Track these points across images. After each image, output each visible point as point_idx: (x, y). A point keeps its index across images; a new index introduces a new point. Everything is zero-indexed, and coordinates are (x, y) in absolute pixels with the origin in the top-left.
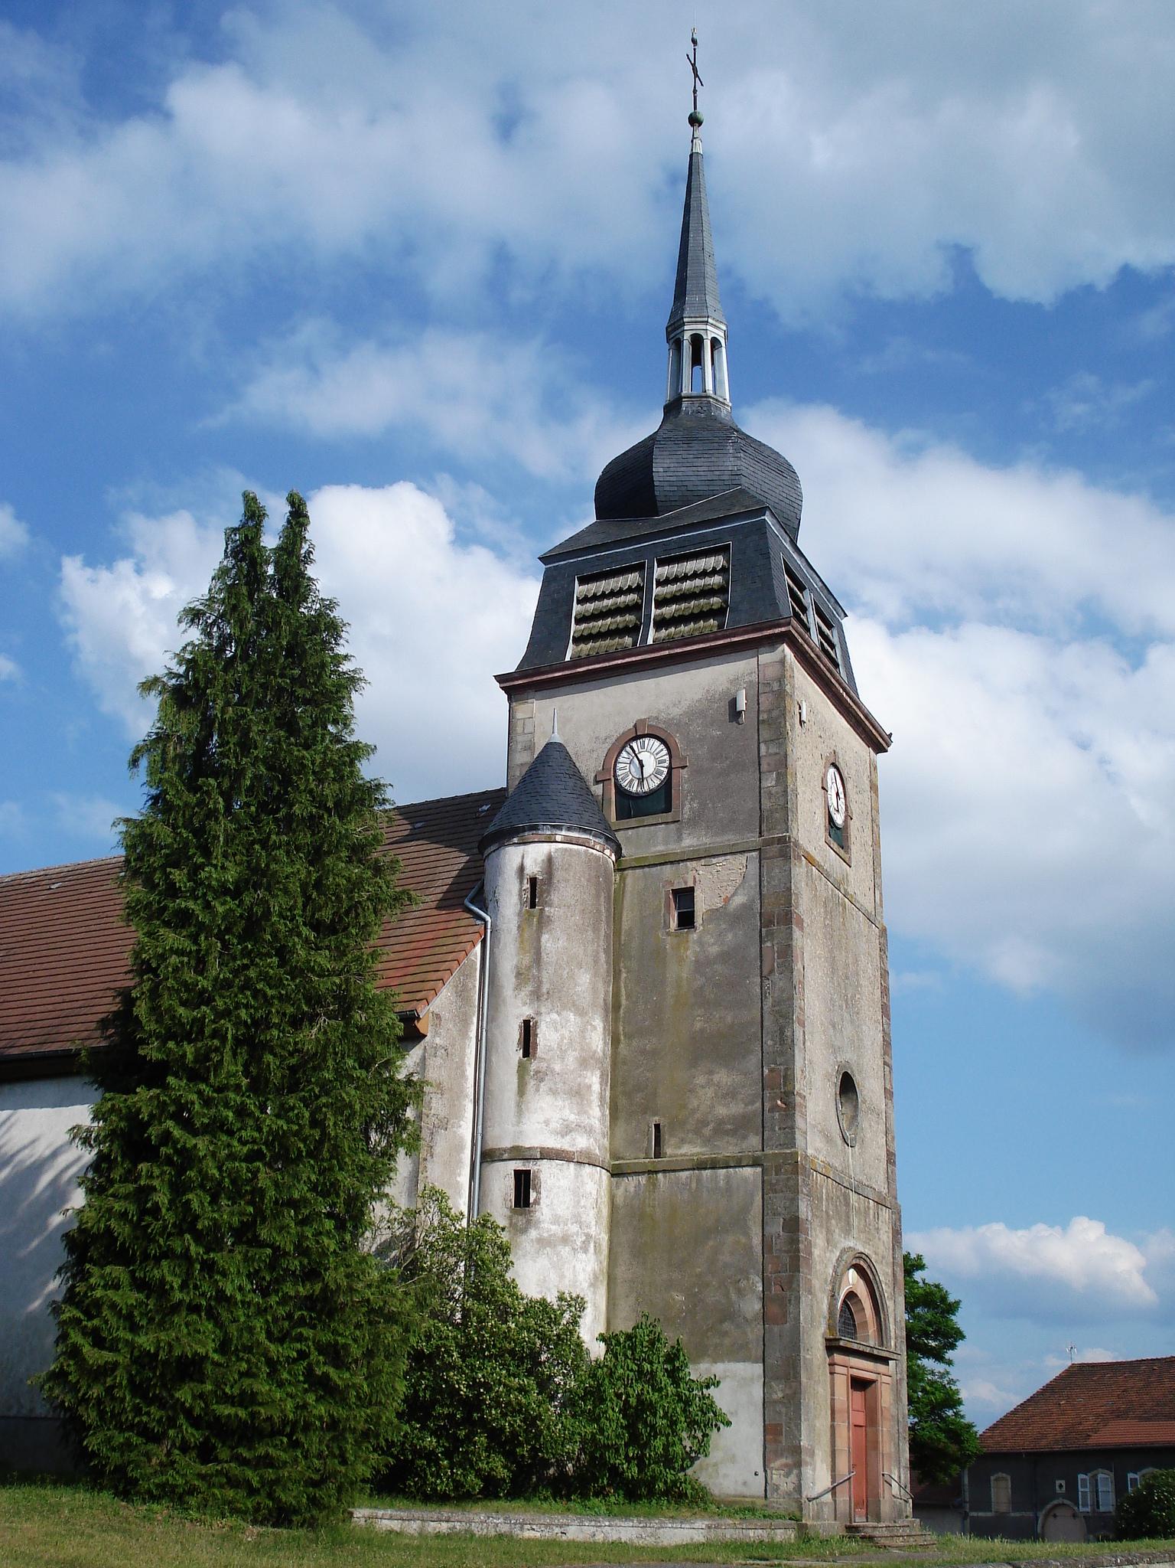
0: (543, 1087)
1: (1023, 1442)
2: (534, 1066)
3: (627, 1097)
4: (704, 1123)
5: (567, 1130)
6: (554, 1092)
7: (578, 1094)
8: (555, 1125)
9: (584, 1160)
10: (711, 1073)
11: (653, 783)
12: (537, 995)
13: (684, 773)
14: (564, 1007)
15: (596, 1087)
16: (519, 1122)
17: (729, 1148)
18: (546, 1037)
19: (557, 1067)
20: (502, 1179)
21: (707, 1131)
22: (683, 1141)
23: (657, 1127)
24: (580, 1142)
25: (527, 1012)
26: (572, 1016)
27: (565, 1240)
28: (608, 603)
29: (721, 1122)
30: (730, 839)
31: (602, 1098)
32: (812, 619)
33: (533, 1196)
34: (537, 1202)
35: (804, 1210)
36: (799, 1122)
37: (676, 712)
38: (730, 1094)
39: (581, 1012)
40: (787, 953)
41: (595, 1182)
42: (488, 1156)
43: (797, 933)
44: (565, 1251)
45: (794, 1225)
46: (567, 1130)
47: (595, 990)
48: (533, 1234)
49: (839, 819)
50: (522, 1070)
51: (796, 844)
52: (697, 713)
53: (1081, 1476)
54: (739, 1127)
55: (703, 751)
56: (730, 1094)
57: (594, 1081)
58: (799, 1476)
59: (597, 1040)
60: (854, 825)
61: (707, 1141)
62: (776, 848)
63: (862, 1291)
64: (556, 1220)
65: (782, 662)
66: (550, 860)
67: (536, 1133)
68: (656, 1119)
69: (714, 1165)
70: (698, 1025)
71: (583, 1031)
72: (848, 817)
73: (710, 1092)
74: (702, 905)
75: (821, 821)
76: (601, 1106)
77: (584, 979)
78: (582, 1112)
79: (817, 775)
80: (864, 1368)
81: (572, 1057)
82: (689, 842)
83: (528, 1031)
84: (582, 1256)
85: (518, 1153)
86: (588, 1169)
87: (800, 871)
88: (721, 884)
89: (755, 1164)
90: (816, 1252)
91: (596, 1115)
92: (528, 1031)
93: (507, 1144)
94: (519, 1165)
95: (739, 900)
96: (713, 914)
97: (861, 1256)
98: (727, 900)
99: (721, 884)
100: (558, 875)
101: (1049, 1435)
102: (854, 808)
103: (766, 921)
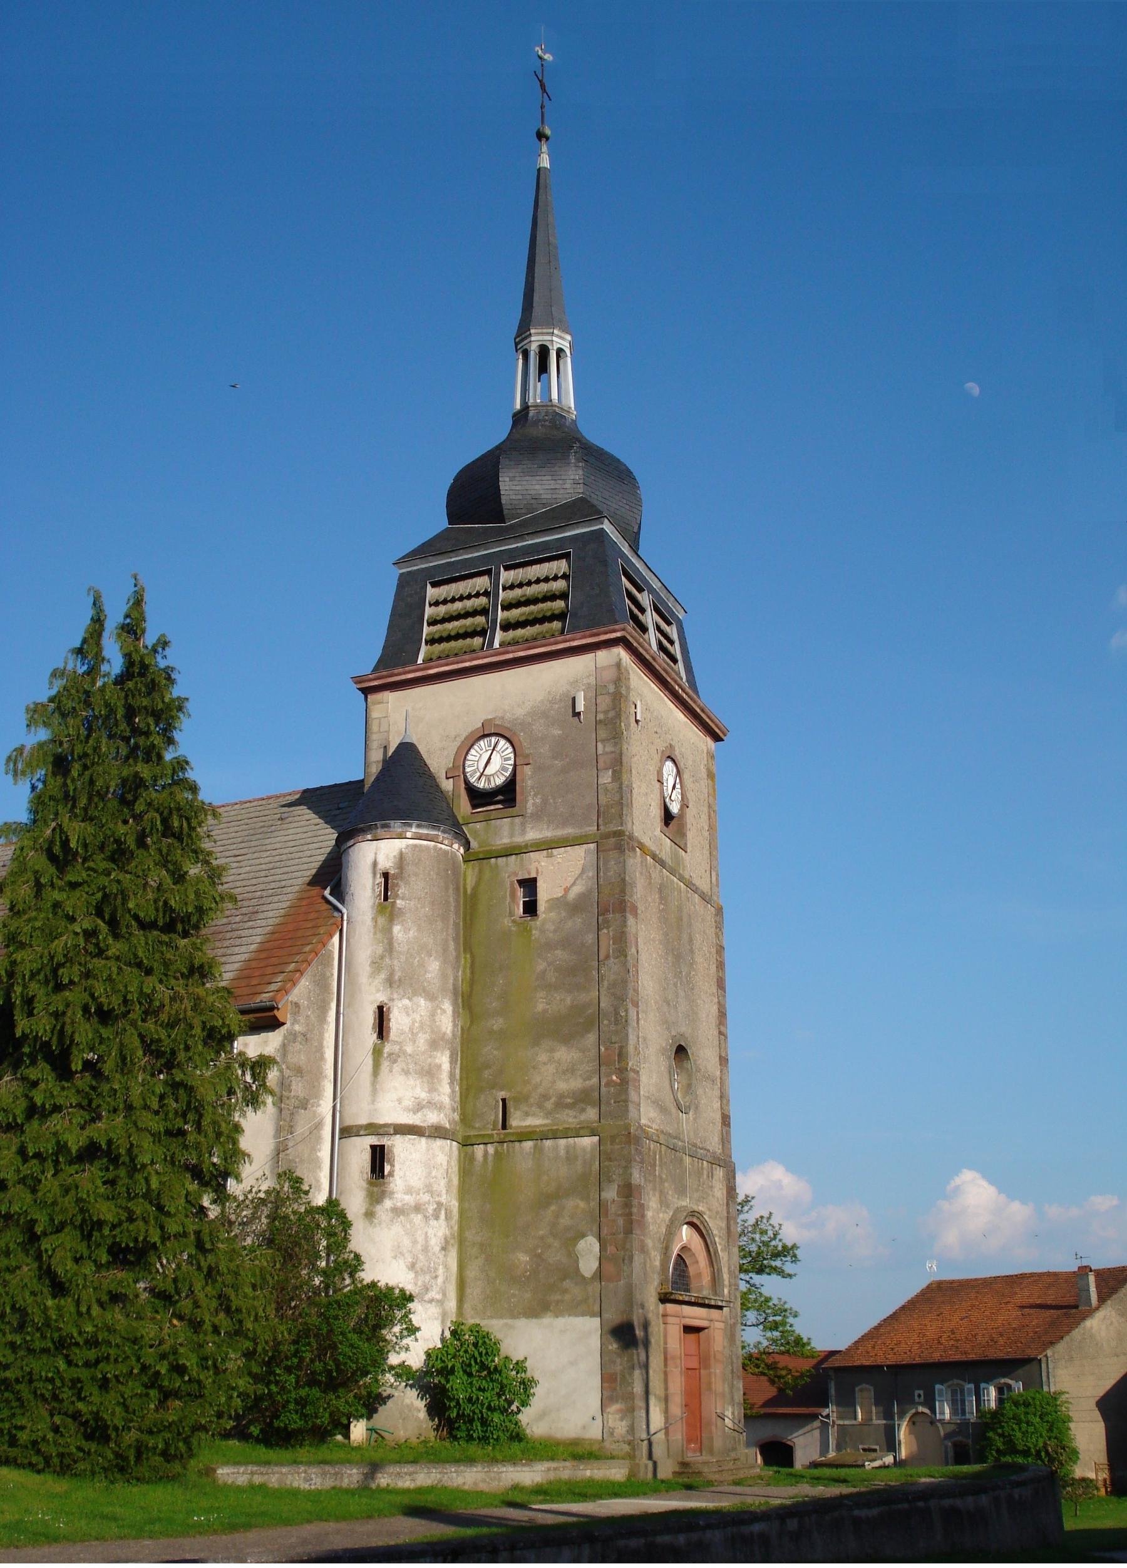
0: (396, 1068)
1: (883, 1356)
2: (388, 1048)
3: (472, 1077)
4: (545, 1097)
5: (419, 1107)
6: (406, 1072)
7: (429, 1073)
8: (408, 1102)
9: (437, 1132)
10: (552, 1050)
11: (499, 781)
12: (390, 982)
13: (528, 770)
14: (415, 993)
15: (446, 1066)
16: (373, 1102)
17: (569, 1118)
18: (398, 1021)
19: (409, 1049)
20: (359, 1152)
21: (549, 1105)
22: (527, 1114)
23: (504, 1100)
24: (432, 1118)
25: (381, 997)
26: (422, 1002)
27: (418, 1208)
28: (458, 605)
29: (561, 1096)
30: (569, 831)
31: (452, 1075)
32: (650, 618)
33: (387, 1168)
34: (391, 1174)
35: (637, 1177)
36: (633, 1096)
37: (520, 712)
38: (571, 1070)
39: (431, 997)
40: (622, 940)
41: (444, 1153)
42: (347, 1132)
43: (631, 921)
44: (418, 1219)
45: (628, 1191)
46: (419, 1107)
47: (444, 976)
48: (388, 1203)
49: (675, 808)
50: (377, 1053)
51: (631, 837)
52: (540, 713)
53: (938, 1387)
54: (582, 1099)
55: (545, 750)
56: (571, 1070)
57: (444, 1060)
58: (633, 1418)
59: (446, 1022)
60: (690, 813)
61: (548, 1114)
62: (612, 840)
63: (697, 1244)
64: (409, 1191)
65: (618, 665)
66: (401, 858)
67: (391, 1111)
68: (502, 1094)
69: (555, 1135)
70: (540, 1007)
71: (433, 1015)
72: (684, 805)
73: (551, 1068)
74: (544, 894)
75: (657, 813)
76: (451, 1083)
77: (434, 966)
78: (432, 1089)
79: (652, 769)
80: (695, 1315)
81: (422, 1039)
82: (532, 835)
83: (382, 1015)
84: (433, 1223)
85: (372, 1129)
86: (439, 1142)
87: (635, 862)
88: (562, 874)
89: (593, 1134)
90: (649, 1214)
91: (446, 1093)
92: (382, 1015)
93: (363, 1121)
94: (374, 1140)
95: (577, 890)
96: (555, 903)
97: (693, 1213)
98: (567, 890)
99: (562, 874)
100: (410, 869)
101: (907, 1348)
102: (691, 796)
103: (602, 911)
